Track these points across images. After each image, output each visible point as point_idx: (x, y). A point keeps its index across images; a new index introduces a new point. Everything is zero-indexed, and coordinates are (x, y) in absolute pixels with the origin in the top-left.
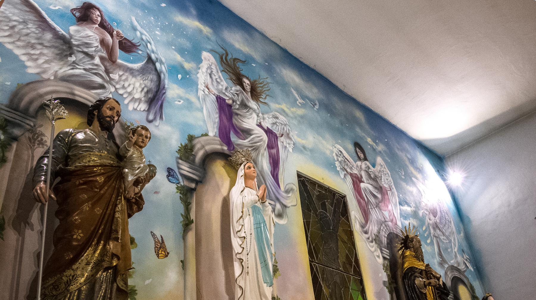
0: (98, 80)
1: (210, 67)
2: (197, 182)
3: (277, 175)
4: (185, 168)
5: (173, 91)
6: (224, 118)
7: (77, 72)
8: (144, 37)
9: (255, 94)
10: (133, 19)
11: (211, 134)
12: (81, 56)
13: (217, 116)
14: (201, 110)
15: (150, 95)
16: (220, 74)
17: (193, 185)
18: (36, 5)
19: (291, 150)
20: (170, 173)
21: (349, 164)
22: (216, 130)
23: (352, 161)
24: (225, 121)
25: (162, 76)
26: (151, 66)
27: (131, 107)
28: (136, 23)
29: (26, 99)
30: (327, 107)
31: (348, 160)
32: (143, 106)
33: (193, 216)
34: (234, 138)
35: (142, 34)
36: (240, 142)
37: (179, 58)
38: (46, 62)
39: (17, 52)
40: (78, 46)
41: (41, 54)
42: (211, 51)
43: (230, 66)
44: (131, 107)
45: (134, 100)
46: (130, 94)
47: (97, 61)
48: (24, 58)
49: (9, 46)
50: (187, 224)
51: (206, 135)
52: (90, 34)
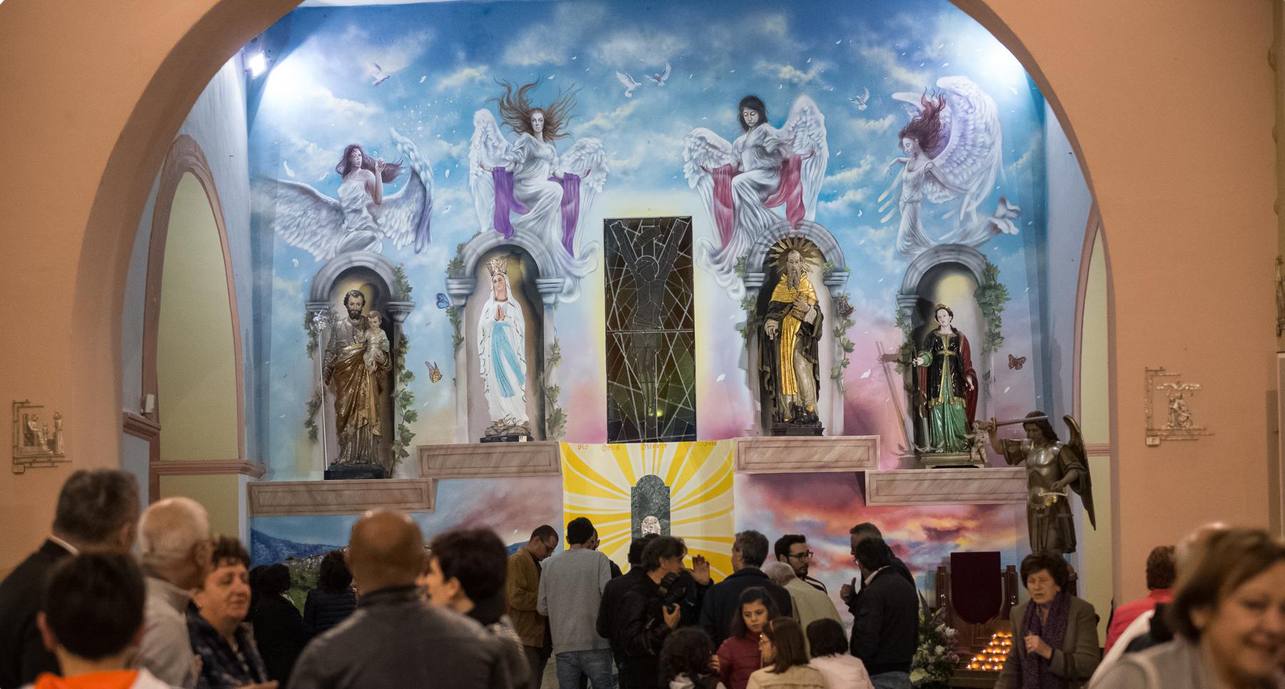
0: (368, 234)
1: (485, 132)
2: (467, 296)
3: (571, 240)
4: (456, 287)
5: (440, 197)
6: (502, 196)
7: (351, 236)
8: (406, 148)
9: (549, 130)
10: (392, 129)
11: (484, 230)
12: (352, 215)
13: (493, 199)
14: (473, 205)
15: (417, 220)
16: (499, 132)
17: (463, 302)
18: (309, 186)
19: (599, 189)
20: (440, 298)
21: (716, 152)
22: (491, 220)
23: (725, 142)
24: (504, 201)
25: (428, 187)
26: (416, 181)
27: (399, 247)
28: (395, 134)
29: (320, 288)
30: (688, 64)
31: (714, 147)
32: (411, 237)
33: (463, 334)
34: (514, 219)
35: (403, 144)
36: (523, 218)
37: (445, 146)
38: (328, 242)
39: (306, 247)
40: (347, 207)
41: (323, 237)
42: (485, 105)
43: (512, 108)
44: (399, 247)
45: (402, 236)
46: (397, 231)
47: (365, 213)
48: (311, 250)
49: (300, 246)
50: (458, 341)
51: (479, 233)
52: (356, 183)
